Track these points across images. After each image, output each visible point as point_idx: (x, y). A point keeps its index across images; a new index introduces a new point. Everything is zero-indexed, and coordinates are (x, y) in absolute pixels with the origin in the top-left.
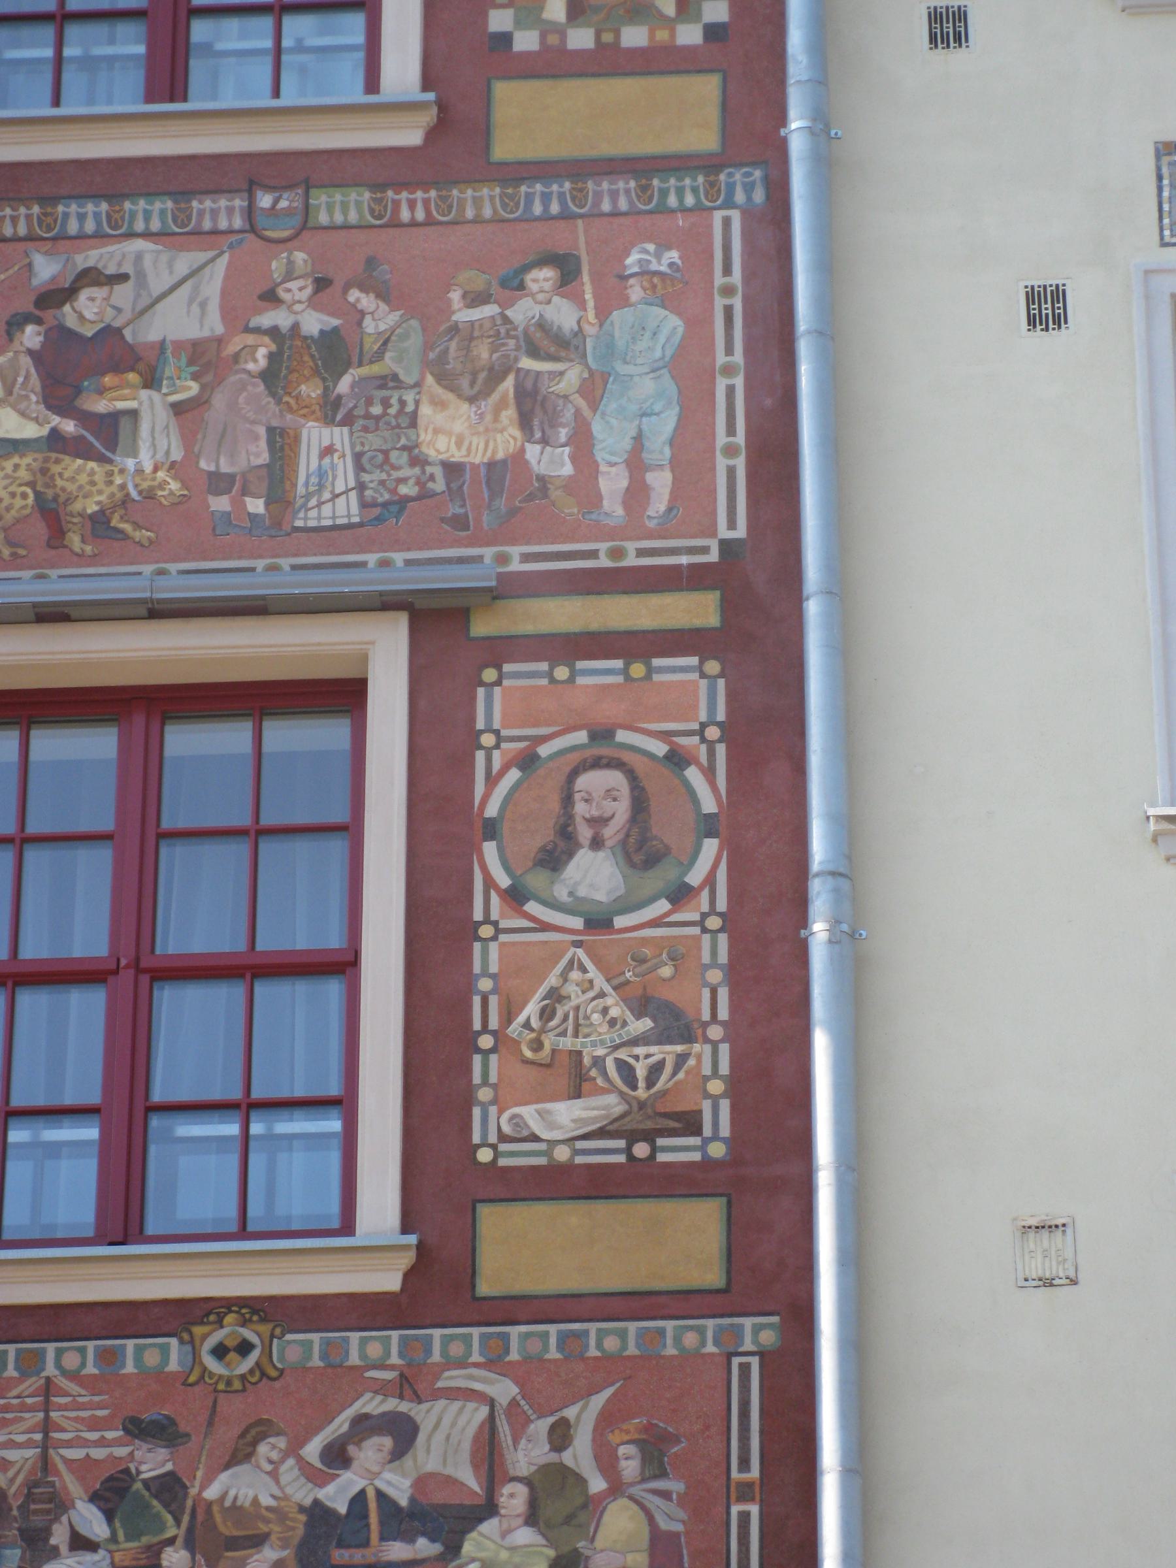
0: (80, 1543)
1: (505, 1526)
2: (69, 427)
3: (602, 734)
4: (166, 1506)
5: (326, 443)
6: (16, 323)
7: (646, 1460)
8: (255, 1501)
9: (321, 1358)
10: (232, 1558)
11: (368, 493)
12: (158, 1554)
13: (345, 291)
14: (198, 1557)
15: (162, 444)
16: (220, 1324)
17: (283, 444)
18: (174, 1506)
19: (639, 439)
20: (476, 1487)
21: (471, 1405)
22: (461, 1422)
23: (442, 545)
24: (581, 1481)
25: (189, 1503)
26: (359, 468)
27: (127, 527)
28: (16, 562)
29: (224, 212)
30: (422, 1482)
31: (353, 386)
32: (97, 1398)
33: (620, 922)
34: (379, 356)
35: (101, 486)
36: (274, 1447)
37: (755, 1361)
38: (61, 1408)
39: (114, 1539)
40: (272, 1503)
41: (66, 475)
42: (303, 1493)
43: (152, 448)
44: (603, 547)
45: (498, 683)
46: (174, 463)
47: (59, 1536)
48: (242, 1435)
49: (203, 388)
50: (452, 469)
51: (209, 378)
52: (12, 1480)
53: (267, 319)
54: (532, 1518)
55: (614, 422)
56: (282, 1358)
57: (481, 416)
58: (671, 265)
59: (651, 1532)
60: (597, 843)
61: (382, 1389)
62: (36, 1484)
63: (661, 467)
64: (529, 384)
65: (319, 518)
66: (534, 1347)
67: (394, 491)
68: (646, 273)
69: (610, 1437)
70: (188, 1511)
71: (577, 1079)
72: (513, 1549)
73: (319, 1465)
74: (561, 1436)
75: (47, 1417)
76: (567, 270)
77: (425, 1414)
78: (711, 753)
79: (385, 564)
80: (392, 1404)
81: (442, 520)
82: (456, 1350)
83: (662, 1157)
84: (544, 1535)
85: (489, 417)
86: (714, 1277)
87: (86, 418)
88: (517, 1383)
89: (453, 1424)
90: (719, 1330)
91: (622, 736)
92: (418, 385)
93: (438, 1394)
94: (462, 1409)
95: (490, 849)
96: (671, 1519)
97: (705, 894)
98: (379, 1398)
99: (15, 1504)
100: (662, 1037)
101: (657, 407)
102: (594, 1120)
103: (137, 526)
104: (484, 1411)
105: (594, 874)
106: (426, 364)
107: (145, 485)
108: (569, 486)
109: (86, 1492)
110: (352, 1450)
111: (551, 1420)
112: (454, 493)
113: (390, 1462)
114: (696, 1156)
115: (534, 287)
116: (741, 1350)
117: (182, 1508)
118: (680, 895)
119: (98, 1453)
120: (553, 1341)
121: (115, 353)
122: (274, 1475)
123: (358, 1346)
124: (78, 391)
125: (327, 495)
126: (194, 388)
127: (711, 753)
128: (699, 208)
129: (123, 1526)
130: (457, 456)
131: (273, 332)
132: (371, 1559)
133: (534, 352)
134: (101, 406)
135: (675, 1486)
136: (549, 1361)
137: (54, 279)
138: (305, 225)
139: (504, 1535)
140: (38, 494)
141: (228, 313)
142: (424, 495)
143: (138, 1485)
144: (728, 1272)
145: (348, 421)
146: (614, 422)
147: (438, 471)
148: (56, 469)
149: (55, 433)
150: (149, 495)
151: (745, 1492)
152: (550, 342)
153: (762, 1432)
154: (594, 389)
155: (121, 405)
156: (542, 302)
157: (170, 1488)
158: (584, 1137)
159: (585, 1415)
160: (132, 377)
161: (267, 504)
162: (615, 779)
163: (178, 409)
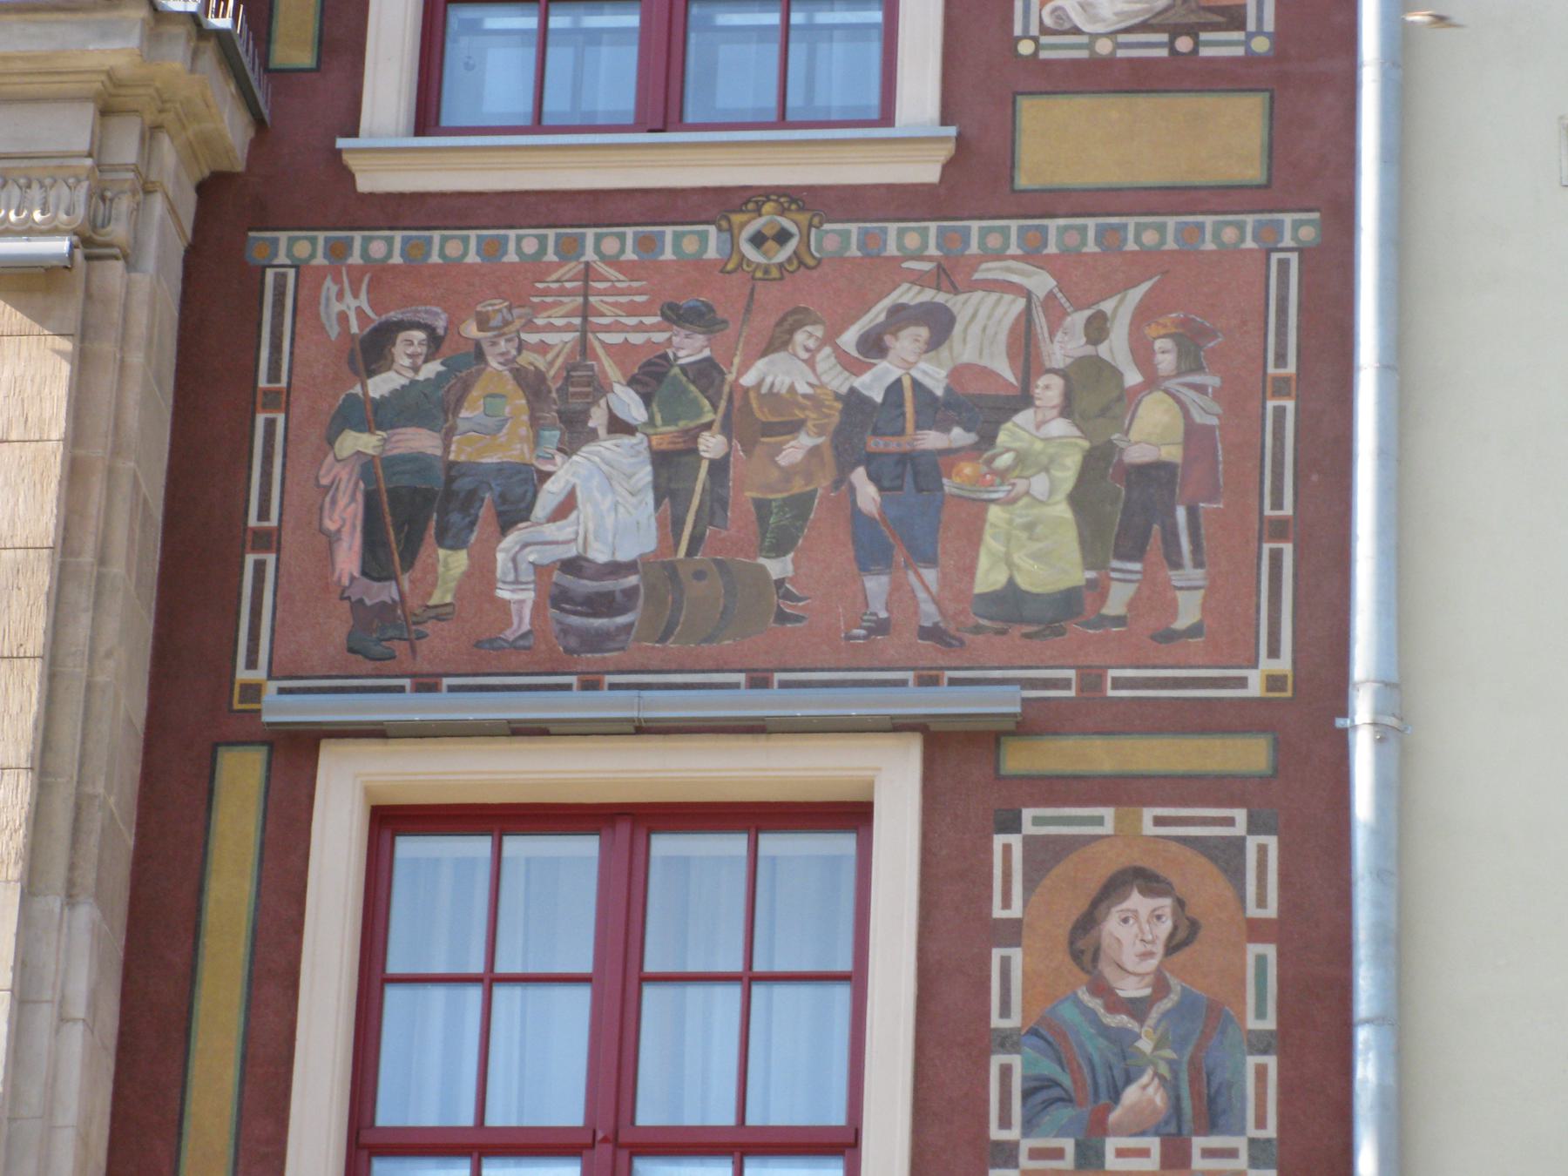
0: (618, 426)
1: (1040, 417)
4: (703, 391)
7: (1182, 354)
8: (792, 389)
9: (859, 249)
10: (768, 444)
12: (695, 438)
14: (735, 442)
16: (758, 212)
18: (711, 392)
20: (1012, 379)
21: (1008, 297)
24: (1117, 374)
25: (726, 389)
30: (957, 373)
32: (635, 284)
36: (811, 335)
37: (1294, 258)
38: (600, 293)
39: (651, 421)
40: (809, 390)
42: (839, 381)
47: (598, 419)
52: (551, 364)
56: (820, 248)
59: (1186, 425)
61: (919, 280)
62: (575, 368)
66: (1072, 239)
69: (1147, 331)
70: (725, 397)
72: (1047, 440)
73: (855, 353)
74: (1097, 329)
75: (586, 302)
80: (928, 295)
82: (994, 241)
83: (1205, 52)
84: (1077, 426)
86: (1253, 172)
88: (1054, 276)
89: (989, 317)
90: (1259, 226)
96: (1207, 414)
98: (917, 288)
99: (554, 386)
104: (1021, 303)
109: (624, 375)
110: (888, 339)
111: (1087, 313)
113: (926, 352)
114: (1239, 51)
116: (1280, 245)
117: (719, 393)
119: (637, 339)
120: (1091, 234)
122: (811, 363)
123: (896, 236)
129: (661, 411)
132: (907, 448)
135: (1212, 381)
136: (1086, 254)
139: (1038, 427)
143: (676, 370)
144: (1270, 168)
151: (1282, 387)
153: (1299, 328)
157: (707, 374)
158: (1127, 30)
159: (1122, 309)
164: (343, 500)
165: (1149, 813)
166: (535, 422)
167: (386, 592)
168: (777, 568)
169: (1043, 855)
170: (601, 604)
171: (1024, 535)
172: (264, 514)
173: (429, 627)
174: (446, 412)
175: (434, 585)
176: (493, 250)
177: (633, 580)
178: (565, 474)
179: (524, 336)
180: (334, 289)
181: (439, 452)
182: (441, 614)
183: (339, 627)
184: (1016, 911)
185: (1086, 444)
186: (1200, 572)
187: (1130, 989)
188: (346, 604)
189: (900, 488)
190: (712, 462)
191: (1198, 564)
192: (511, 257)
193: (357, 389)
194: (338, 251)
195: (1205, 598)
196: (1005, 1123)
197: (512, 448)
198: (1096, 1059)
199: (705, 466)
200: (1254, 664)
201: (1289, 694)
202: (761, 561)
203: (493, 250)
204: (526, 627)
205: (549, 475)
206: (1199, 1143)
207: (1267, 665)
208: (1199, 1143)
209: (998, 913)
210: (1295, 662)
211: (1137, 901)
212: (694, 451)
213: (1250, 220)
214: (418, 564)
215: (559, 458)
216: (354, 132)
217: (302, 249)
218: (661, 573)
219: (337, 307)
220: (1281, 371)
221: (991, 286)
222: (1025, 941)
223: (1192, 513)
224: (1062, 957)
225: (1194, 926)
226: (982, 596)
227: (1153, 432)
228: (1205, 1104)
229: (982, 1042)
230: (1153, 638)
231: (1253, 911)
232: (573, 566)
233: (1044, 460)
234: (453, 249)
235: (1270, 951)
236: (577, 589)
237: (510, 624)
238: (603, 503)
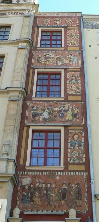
0: (46, 111)
17: (57, 62)
29: (54, 52)
43: (50, 62)
47: (45, 111)
50: (66, 63)
53: (56, 56)
74: (72, 107)
76: (72, 55)
86: (80, 100)
96: (79, 111)
105: (74, 81)
118: (78, 82)
121: (48, 58)
123: (61, 102)
138: (58, 52)
151: (82, 110)
152: (70, 58)
154: (73, 60)
157: (51, 109)
159: (74, 106)
165: (76, 131)
168: (55, 118)
169: (70, 133)
170: (46, 120)
172: (27, 115)
176: (39, 103)
178: (43, 113)
184: (69, 136)
187: (76, 140)
194: (31, 103)
196: (69, 147)
197: (41, 112)
203: (39, 103)
217: (29, 102)
218: (49, 118)
221: (67, 105)
223: (78, 116)
227: (76, 112)
228: (80, 146)
229: (67, 143)
232: (44, 118)
236: (45, 120)
238: (46, 115)
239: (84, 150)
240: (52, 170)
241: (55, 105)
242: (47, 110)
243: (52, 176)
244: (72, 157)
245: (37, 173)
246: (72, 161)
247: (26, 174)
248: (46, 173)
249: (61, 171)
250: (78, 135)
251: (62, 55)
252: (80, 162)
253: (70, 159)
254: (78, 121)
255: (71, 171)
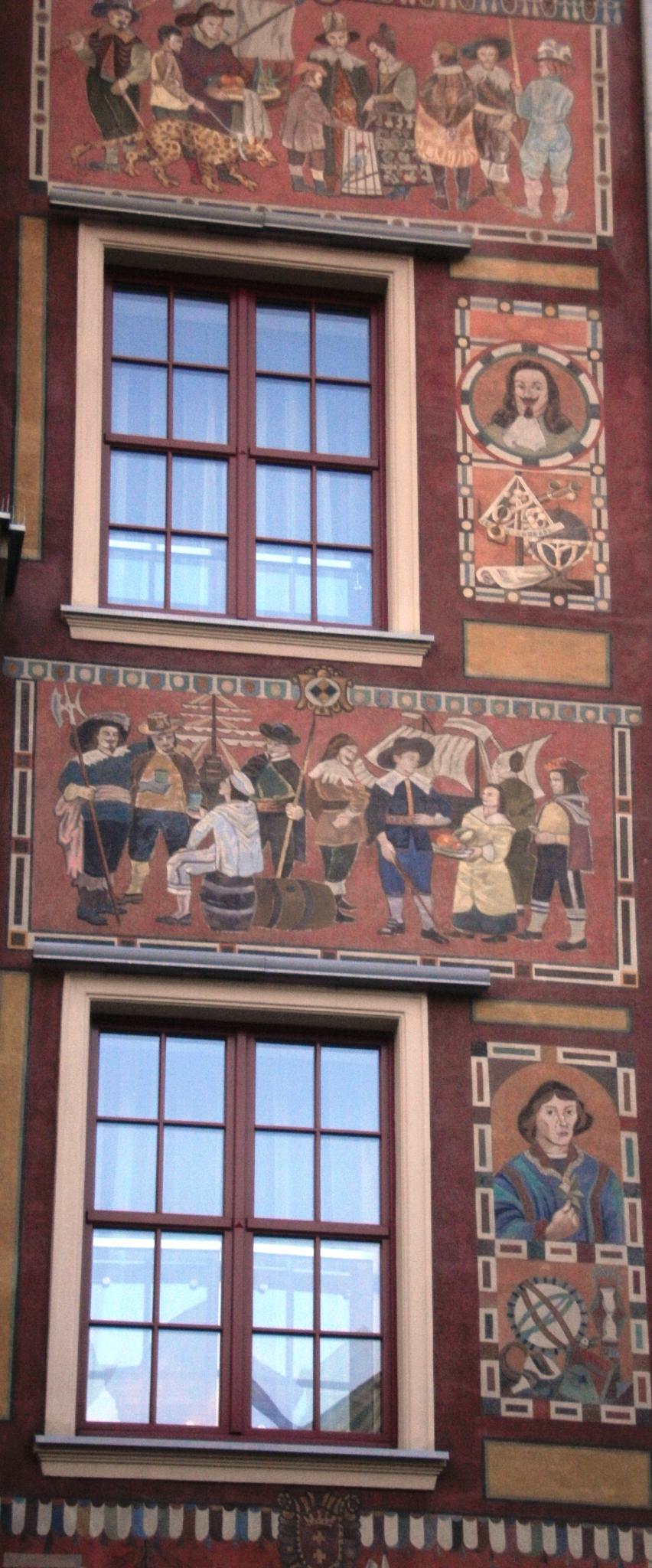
0: (237, 795)
2: (201, 106)
3: (530, 347)
4: (287, 779)
5: (359, 141)
6: (164, 33)
7: (566, 782)
8: (340, 781)
11: (386, 177)
12: (284, 807)
13: (368, 43)
15: (259, 127)
16: (315, 675)
17: (333, 138)
19: (548, 166)
21: (464, 740)
22: (460, 747)
23: (433, 217)
24: (530, 791)
26: (380, 160)
27: (240, 177)
28: (171, 188)
30: (437, 781)
31: (375, 106)
33: (543, 463)
34: (390, 89)
35: (222, 147)
37: (628, 732)
38: (222, 714)
39: (257, 795)
40: (349, 783)
41: (201, 137)
42: (368, 781)
44: (528, 231)
45: (468, 307)
46: (266, 141)
47: (224, 790)
48: (331, 742)
49: (283, 93)
50: (437, 170)
51: (286, 88)
52: (195, 754)
54: (502, 809)
55: (533, 153)
57: (453, 138)
58: (566, 56)
60: (529, 414)
61: (412, 724)
63: (561, 185)
64: (481, 121)
65: (357, 189)
66: (500, 709)
67: (402, 178)
68: (550, 59)
71: (520, 554)
72: (491, 825)
74: (517, 763)
77: (438, 741)
78: (594, 367)
79: (398, 223)
80: (418, 734)
81: (432, 201)
82: (454, 705)
83: (571, 606)
85: (458, 139)
86: (602, 679)
87: (211, 102)
90: (607, 711)
91: (542, 350)
92: (414, 112)
93: (444, 731)
94: (458, 742)
95: (466, 410)
97: (592, 452)
99: (198, 768)
100: (569, 536)
101: (559, 146)
102: (531, 580)
103: (246, 177)
104: (472, 744)
105: (528, 433)
106: (419, 99)
107: (249, 152)
108: (507, 190)
110: (396, 758)
111: (511, 753)
112: (439, 185)
114: (592, 608)
115: (483, 58)
117: (297, 781)
118: (578, 451)
119: (246, 744)
120: (511, 707)
122: (350, 767)
124: (206, 84)
125: (361, 175)
126: (276, 93)
127: (594, 367)
128: (581, 21)
130: (439, 161)
131: (325, 64)
132: (410, 823)
133: (484, 100)
134: (220, 95)
135: (583, 799)
137: (187, 7)
140: (184, 148)
141: (296, 45)
142: (420, 183)
143: (270, 765)
145: (372, 128)
146: (533, 153)
147: (428, 169)
148: (194, 133)
149: (192, 107)
150: (252, 158)
151: (624, 806)
154: (521, 128)
155: (232, 97)
156: (486, 68)
157: (289, 769)
159: (531, 752)
160: (239, 80)
161: (325, 176)
162: (538, 376)
163: (268, 105)
164: (71, 826)
165: (560, 1051)
166: (187, 789)
167: (101, 884)
168: (336, 888)
169: (501, 1071)
170: (233, 901)
171: (480, 881)
172: (21, 830)
173: (127, 907)
174: (132, 779)
175: (129, 882)
176: (155, 682)
177: (250, 888)
178: (207, 822)
179: (178, 736)
180: (59, 696)
181: (128, 801)
182: (135, 899)
183: (71, 903)
185: (514, 830)
186: (582, 911)
187: (555, 1153)
188: (75, 889)
189: (407, 847)
190: (295, 822)
191: (582, 906)
192: (168, 687)
193: (76, 759)
194: (61, 674)
195: (586, 927)
196: (486, 1229)
197: (172, 802)
198: (537, 1193)
199: (290, 824)
200: (616, 967)
201: (636, 986)
202: (327, 883)
203: (155, 682)
204: (187, 912)
205: (196, 821)
206: (599, 1248)
207: (623, 968)
208: (599, 1248)
209: (476, 1103)
210: (640, 968)
211: (556, 1102)
212: (283, 814)
213: (601, 707)
214: (119, 869)
215: (202, 811)
216: (69, 603)
217: (38, 670)
218: (267, 887)
219: (62, 708)
220: (623, 797)
221: (454, 732)
222: (492, 1120)
223: (577, 875)
224: (514, 1132)
225: (589, 1120)
226: (457, 915)
227: (552, 825)
228: (600, 1225)
230: (558, 947)
231: (623, 1112)
232: (214, 877)
233: (490, 837)
234: (132, 679)
235: (634, 1136)
236: (216, 891)
237: (176, 909)
238: (229, 840)
239: (636, 1275)
240: (319, 1490)
241: (326, 729)
242: (246, 786)
243: (320, 1556)
244: (522, 1344)
245: (163, 1523)
246: (524, 1394)
247: (43, 1528)
248: (254, 1520)
249: (408, 1503)
250: (572, 1104)
251: (383, 36)
252: (605, 1408)
253: (495, 1365)
254: (577, 934)
255: (513, 1511)
